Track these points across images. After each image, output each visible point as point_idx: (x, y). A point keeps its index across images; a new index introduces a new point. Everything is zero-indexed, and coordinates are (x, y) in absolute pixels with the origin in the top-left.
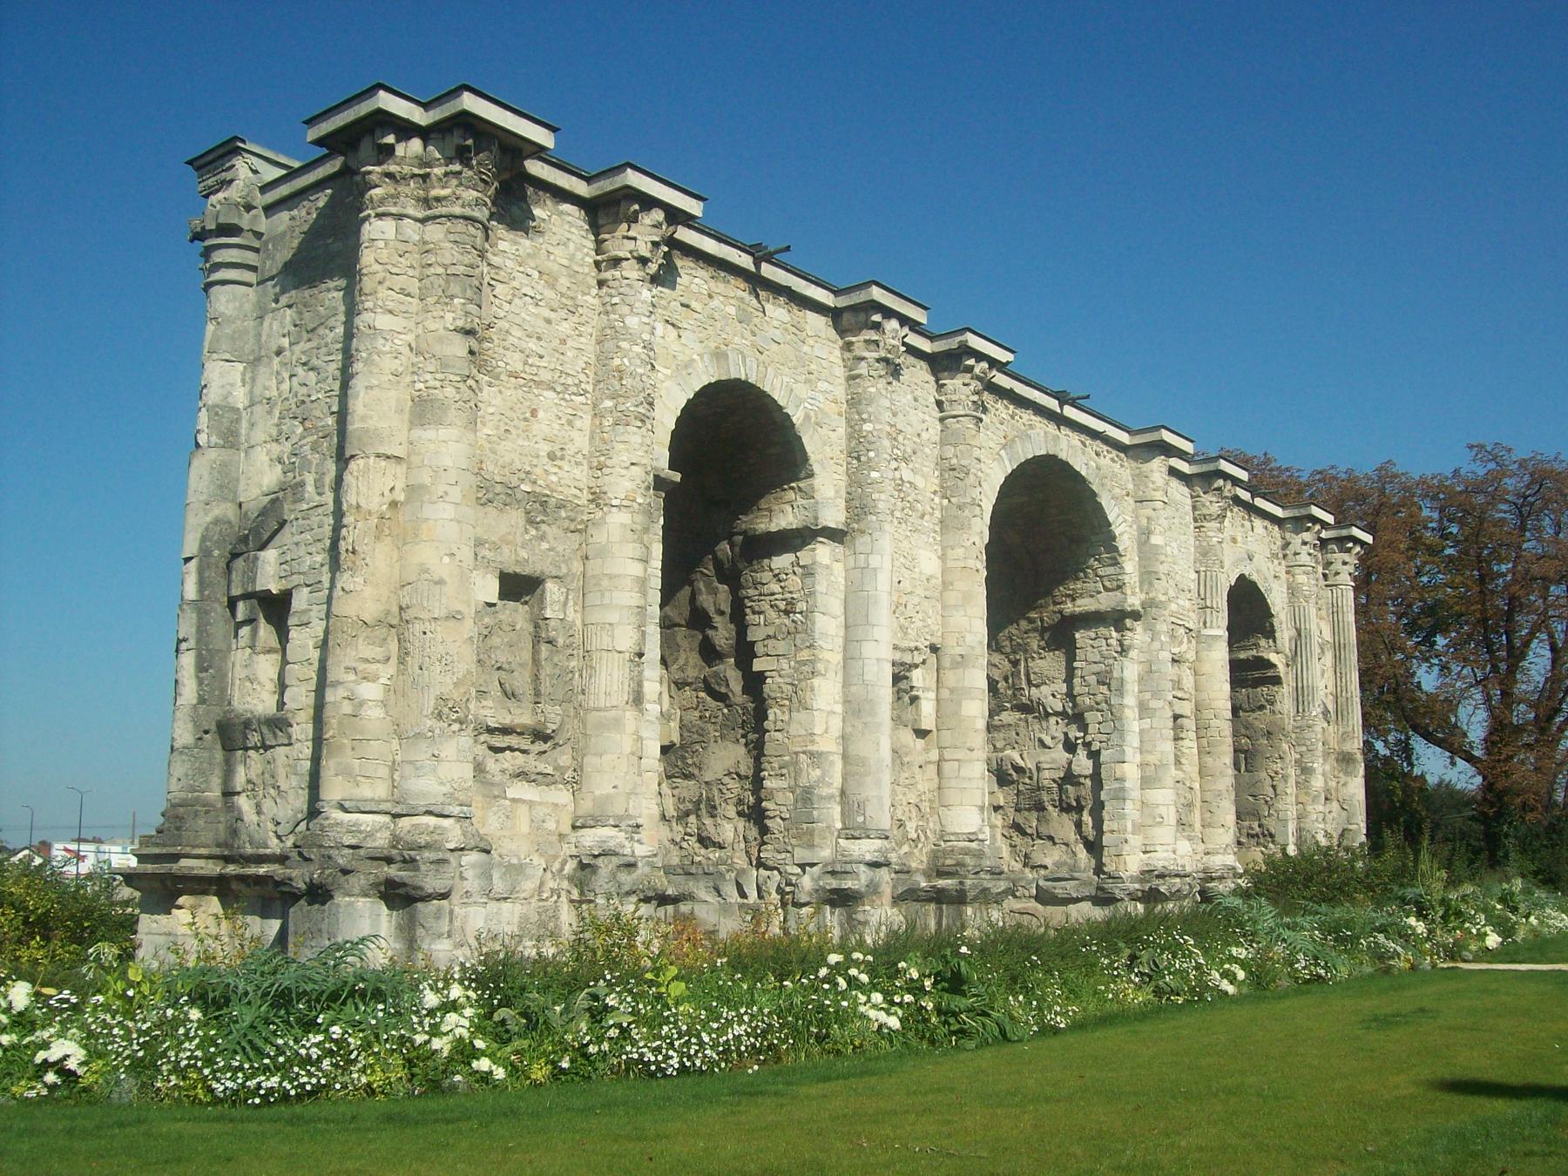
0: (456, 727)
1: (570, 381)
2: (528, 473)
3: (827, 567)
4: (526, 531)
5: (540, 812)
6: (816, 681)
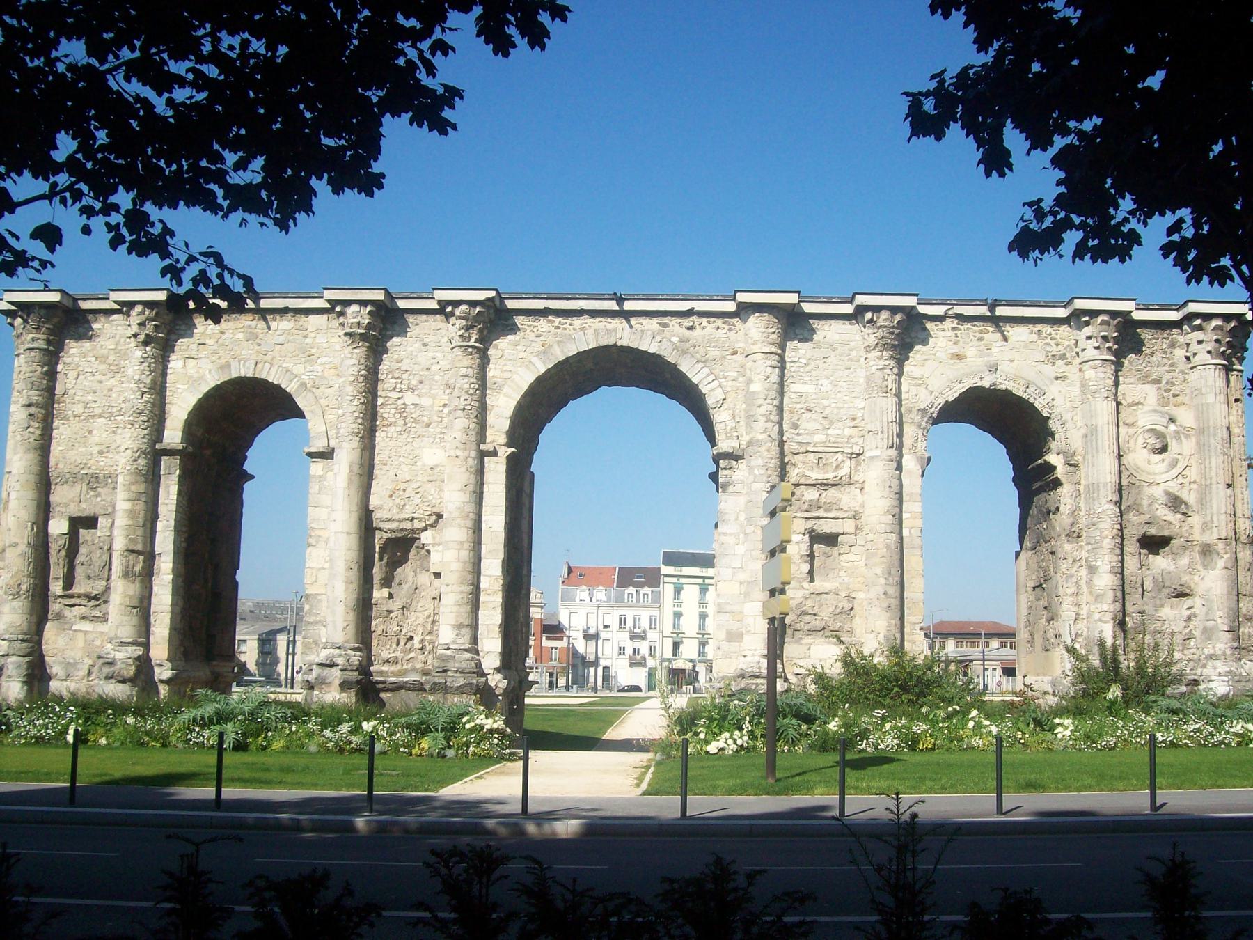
0: (11, 597)
1: (114, 410)
2: (86, 464)
3: (320, 476)
4: (88, 493)
5: (90, 637)
6: (309, 550)
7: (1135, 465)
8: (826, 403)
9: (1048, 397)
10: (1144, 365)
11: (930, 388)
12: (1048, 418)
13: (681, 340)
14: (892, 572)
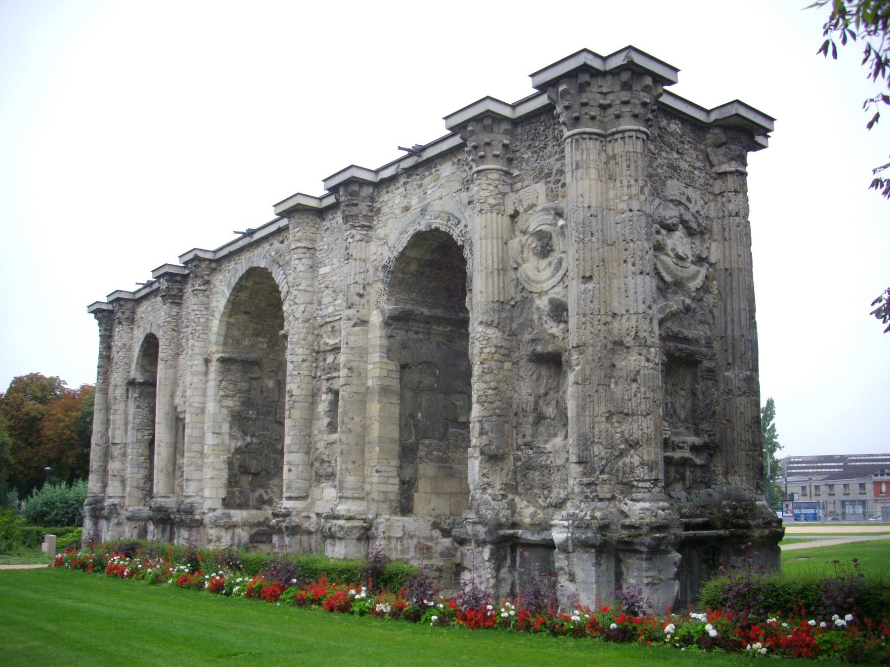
7: (527, 276)
8: (334, 278)
9: (461, 226)
10: (539, 161)
11: (389, 245)
12: (463, 247)
13: (276, 253)
14: (345, 421)
